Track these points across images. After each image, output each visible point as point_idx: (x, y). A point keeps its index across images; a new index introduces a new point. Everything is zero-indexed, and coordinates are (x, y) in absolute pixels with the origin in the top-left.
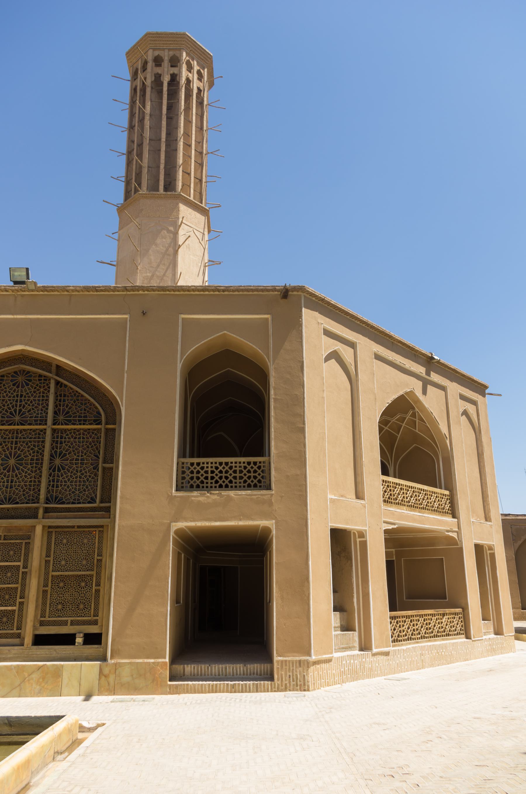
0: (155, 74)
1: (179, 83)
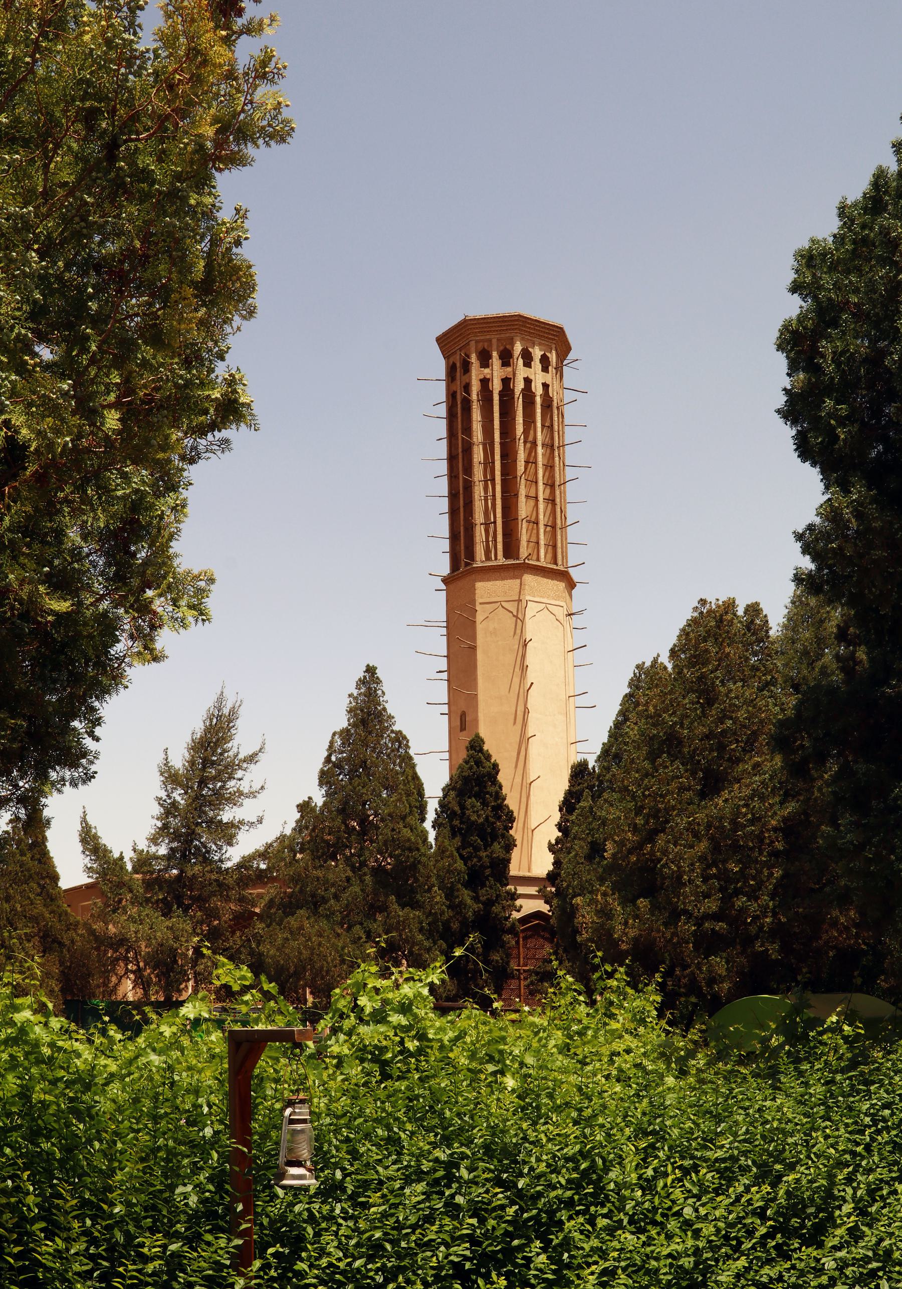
0: (481, 380)
1: (513, 391)
